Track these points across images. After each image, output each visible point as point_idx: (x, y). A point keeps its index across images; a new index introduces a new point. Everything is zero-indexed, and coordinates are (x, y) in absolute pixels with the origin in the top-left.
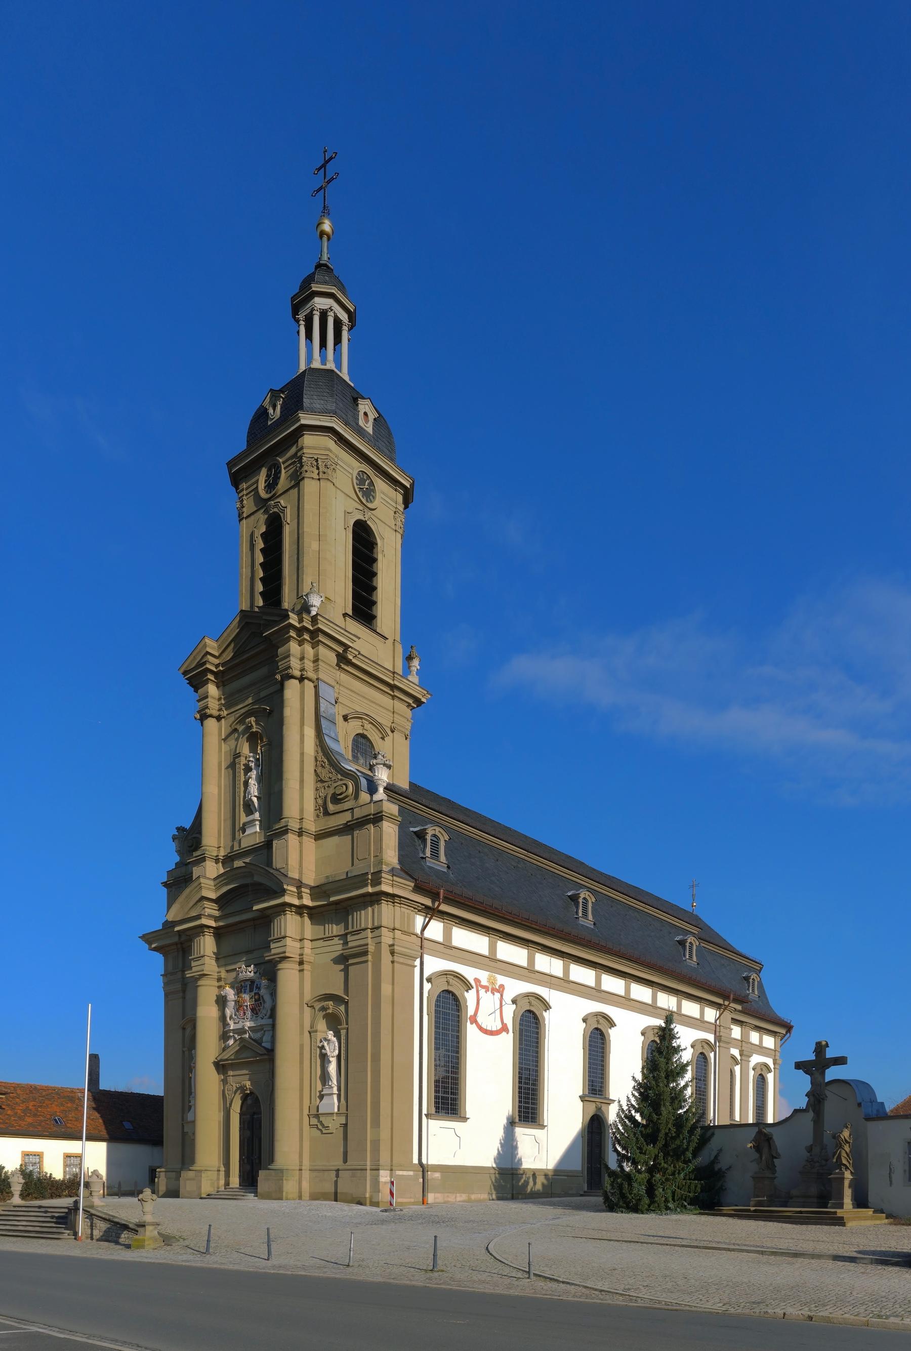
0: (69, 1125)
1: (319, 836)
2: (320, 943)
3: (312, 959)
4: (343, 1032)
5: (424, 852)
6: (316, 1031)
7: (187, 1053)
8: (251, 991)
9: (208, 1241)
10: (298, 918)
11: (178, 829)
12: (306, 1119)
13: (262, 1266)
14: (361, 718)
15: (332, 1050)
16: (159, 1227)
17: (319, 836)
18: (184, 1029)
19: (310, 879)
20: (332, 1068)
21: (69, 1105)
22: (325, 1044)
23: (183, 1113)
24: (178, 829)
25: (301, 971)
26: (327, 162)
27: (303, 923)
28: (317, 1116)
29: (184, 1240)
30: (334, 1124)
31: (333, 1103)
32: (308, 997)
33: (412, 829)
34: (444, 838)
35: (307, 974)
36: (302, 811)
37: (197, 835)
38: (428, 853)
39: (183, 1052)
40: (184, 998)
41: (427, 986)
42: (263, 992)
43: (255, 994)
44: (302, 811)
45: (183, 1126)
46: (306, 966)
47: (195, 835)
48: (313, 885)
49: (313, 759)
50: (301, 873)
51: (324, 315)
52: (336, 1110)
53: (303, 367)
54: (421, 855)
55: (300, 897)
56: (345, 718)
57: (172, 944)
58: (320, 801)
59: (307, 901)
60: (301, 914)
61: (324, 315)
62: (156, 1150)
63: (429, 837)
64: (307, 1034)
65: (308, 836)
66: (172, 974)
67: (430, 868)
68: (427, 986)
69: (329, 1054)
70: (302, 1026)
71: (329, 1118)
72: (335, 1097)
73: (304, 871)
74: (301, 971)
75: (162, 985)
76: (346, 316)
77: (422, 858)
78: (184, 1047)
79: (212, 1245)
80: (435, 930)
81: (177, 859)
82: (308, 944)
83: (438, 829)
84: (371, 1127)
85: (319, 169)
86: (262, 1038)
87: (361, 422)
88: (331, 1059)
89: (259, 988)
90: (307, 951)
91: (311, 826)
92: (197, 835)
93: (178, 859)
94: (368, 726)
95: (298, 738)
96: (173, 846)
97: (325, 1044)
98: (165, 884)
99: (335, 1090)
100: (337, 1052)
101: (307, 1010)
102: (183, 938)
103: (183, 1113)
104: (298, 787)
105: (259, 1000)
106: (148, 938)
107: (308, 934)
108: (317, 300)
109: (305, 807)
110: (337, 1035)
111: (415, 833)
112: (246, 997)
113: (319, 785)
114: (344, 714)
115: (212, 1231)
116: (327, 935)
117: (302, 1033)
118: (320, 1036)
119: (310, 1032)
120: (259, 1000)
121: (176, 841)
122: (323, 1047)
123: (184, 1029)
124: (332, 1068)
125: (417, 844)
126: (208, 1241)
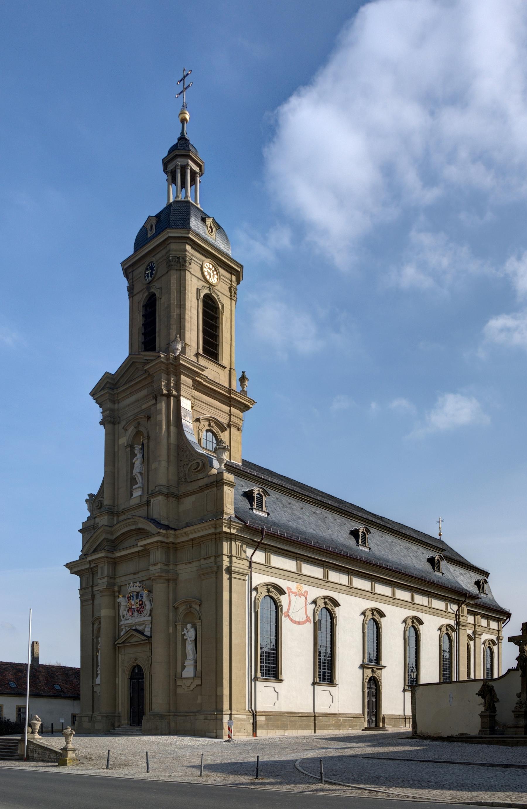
0: (19, 687)
7: (95, 640)
8: (137, 598)
9: (108, 760)
11: (89, 495)
13: (143, 775)
16: (77, 752)
18: (93, 624)
21: (20, 674)
23: (93, 679)
24: (89, 495)
26: (185, 77)
29: (93, 760)
37: (102, 499)
39: (93, 639)
40: (93, 604)
42: (145, 599)
43: (140, 601)
45: (93, 687)
47: (100, 499)
57: (84, 570)
62: (76, 702)
66: (85, 588)
75: (79, 596)
76: (198, 169)
78: (93, 636)
79: (110, 763)
81: (89, 514)
86: (144, 629)
89: (142, 597)
92: (102, 499)
93: (89, 514)
96: (86, 506)
98: (80, 531)
102: (93, 565)
103: (93, 679)
105: (142, 604)
106: (70, 566)
108: (179, 160)
112: (133, 602)
115: (111, 754)
120: (142, 604)
121: (88, 503)
123: (93, 624)
126: (108, 760)
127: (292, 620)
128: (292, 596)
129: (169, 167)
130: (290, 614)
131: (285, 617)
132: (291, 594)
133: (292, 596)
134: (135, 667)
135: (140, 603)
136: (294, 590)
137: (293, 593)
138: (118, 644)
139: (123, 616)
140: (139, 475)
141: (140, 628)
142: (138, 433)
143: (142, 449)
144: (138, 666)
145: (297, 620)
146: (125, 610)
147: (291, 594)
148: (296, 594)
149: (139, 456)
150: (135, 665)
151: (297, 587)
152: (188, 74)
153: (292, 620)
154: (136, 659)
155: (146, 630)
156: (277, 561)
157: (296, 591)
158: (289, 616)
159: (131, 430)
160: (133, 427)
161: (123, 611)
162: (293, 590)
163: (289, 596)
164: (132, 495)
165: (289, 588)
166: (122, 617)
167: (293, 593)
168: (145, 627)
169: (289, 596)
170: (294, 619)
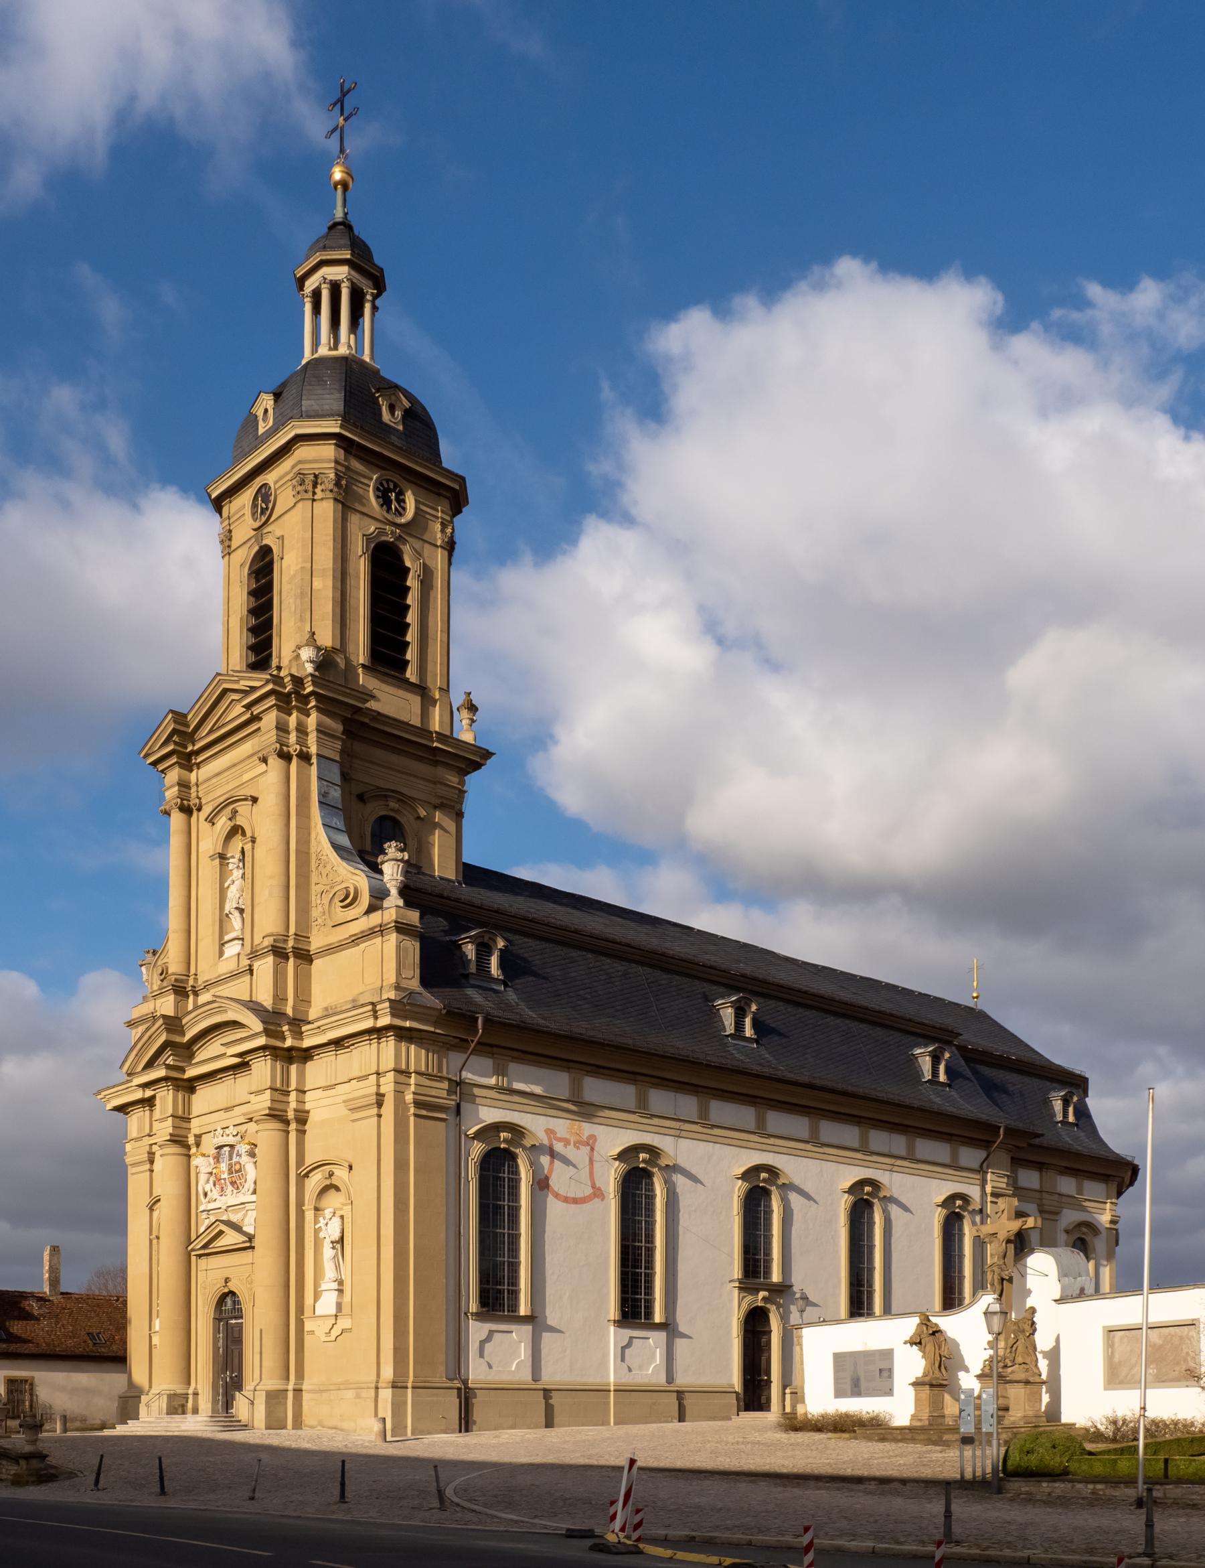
14: (386, 796)
26: (344, 94)
51: (335, 288)
53: (308, 356)
61: (335, 288)
76: (370, 283)
85: (335, 104)
87: (386, 416)
94: (393, 804)
129: (307, 283)
134: (224, 1296)
135: (237, 1167)
137: (560, 1140)
138: (193, 1250)
139: (206, 1194)
140: (237, 914)
141: (235, 1218)
142: (235, 831)
143: (243, 860)
144: (232, 1293)
145: (571, 1195)
146: (208, 1181)
148: (566, 1142)
149: (237, 874)
150: (226, 1290)
152: (349, 91)
154: (227, 1280)
155: (246, 1221)
157: (568, 1136)
159: (223, 823)
160: (224, 819)
161: (203, 1183)
164: (221, 954)
166: (202, 1197)
167: (560, 1140)
168: (245, 1215)
170: (562, 1192)
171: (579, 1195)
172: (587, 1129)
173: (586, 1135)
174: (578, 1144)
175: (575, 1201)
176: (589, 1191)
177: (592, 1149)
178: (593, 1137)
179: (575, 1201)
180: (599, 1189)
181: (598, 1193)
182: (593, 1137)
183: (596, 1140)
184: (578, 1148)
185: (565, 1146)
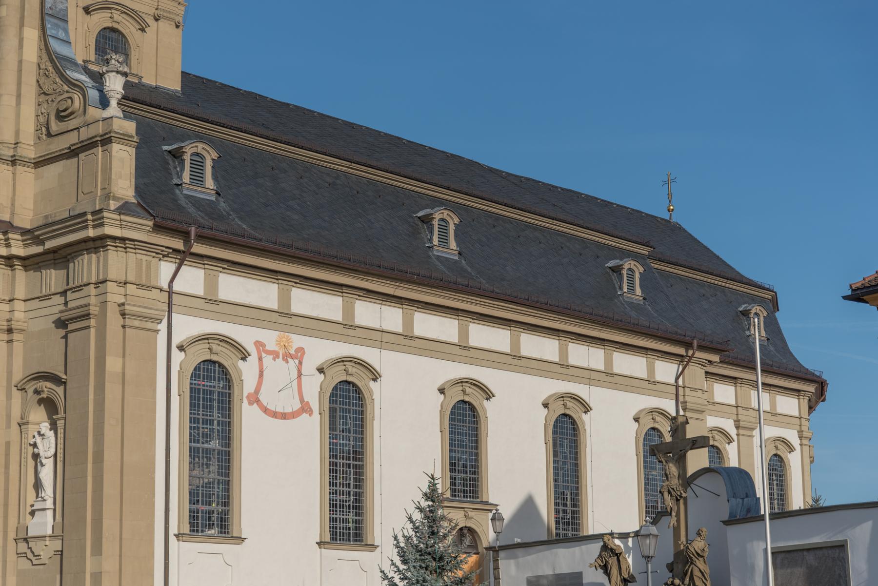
1: (38, 164)
2: (36, 304)
3: (23, 326)
4: (60, 424)
5: (180, 177)
6: (27, 423)
10: (8, 271)
12: (11, 544)
14: (110, 8)
15: (47, 447)
17: (38, 164)
19: (26, 219)
20: (46, 474)
22: (38, 440)
25: (10, 341)
27: (14, 277)
28: (26, 540)
30: (46, 550)
31: (44, 524)
32: (18, 375)
33: (165, 148)
34: (210, 156)
35: (18, 347)
36: (17, 133)
38: (186, 177)
41: (178, 357)
44: (17, 133)
46: (16, 336)
48: (28, 226)
49: (35, 67)
50: (13, 214)
52: (49, 532)
54: (176, 181)
55: (8, 246)
56: (87, 10)
58: (42, 119)
59: (18, 249)
60: (11, 266)
63: (187, 158)
64: (15, 427)
65: (24, 166)
67: (188, 197)
68: (178, 357)
69: (41, 455)
70: (9, 417)
71: (41, 544)
72: (50, 513)
73: (18, 210)
74: (10, 341)
77: (177, 185)
80: (192, 280)
82: (19, 306)
83: (200, 146)
84: (92, 555)
88: (44, 461)
90: (19, 315)
91: (30, 152)
94: (117, 16)
95: (15, 42)
97: (38, 440)
99: (49, 504)
100: (53, 451)
101: (17, 395)
104: (14, 103)
107: (21, 292)
109: (22, 127)
110: (54, 426)
111: (170, 152)
113: (43, 98)
114: (85, 5)
116: (44, 293)
117: (8, 426)
118: (32, 430)
119: (20, 425)
122: (35, 445)
124: (46, 474)
125: (171, 167)
127: (266, 410)
128: (268, 360)
130: (261, 398)
131: (250, 404)
132: (264, 355)
133: (268, 360)
136: (271, 346)
137: (269, 353)
145: (280, 410)
147: (264, 355)
148: (275, 355)
151: (279, 342)
153: (266, 410)
156: (235, 287)
157: (276, 349)
158: (258, 401)
162: (268, 348)
163: (260, 359)
165: (259, 345)
167: (269, 353)
169: (260, 359)
171: (288, 410)
172: (298, 341)
173: (295, 347)
174: (287, 357)
175: (284, 416)
176: (297, 406)
177: (300, 363)
178: (301, 350)
179: (284, 416)
180: (308, 403)
181: (305, 408)
182: (301, 350)
183: (304, 353)
184: (287, 362)
185: (274, 359)
